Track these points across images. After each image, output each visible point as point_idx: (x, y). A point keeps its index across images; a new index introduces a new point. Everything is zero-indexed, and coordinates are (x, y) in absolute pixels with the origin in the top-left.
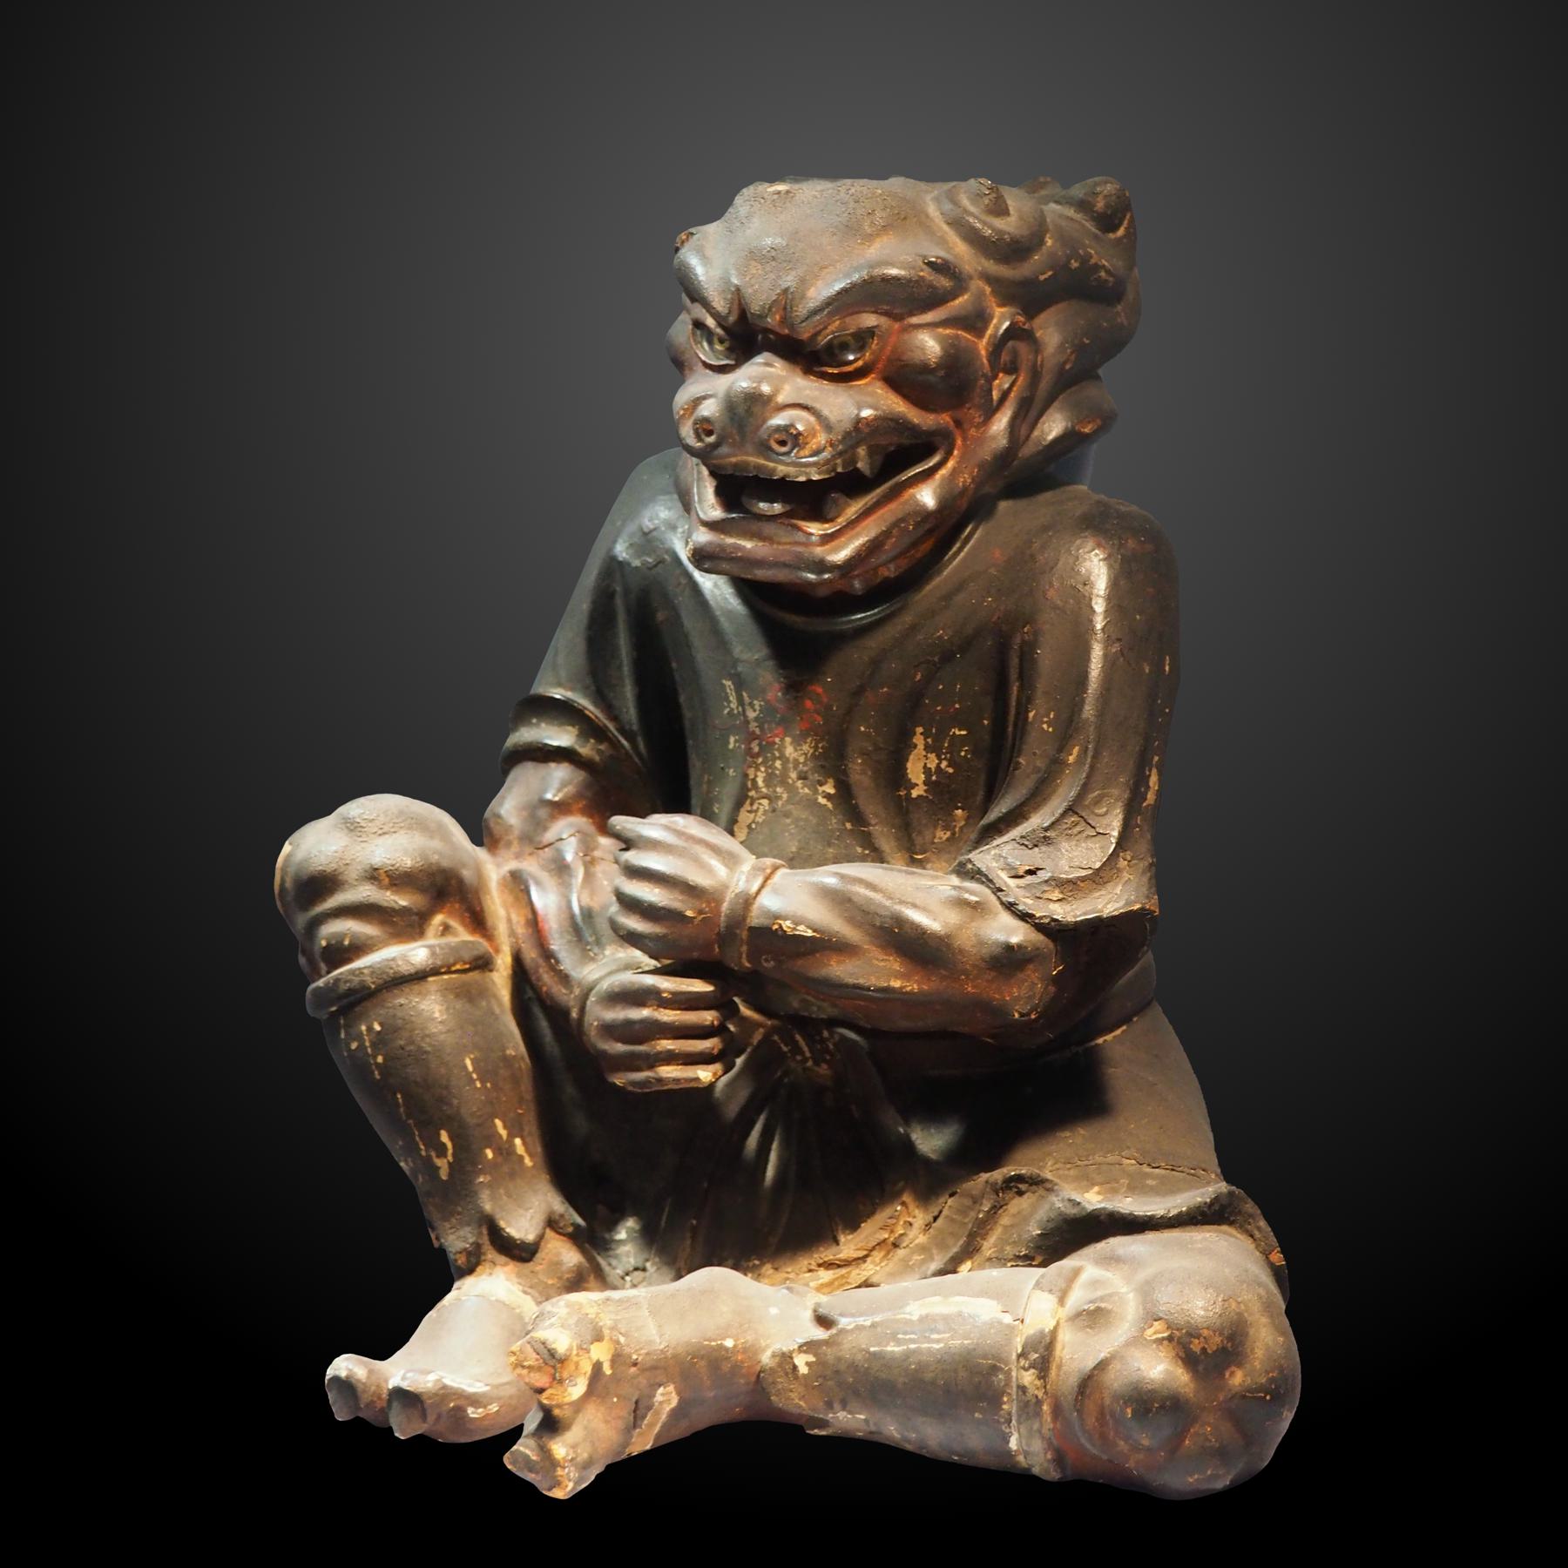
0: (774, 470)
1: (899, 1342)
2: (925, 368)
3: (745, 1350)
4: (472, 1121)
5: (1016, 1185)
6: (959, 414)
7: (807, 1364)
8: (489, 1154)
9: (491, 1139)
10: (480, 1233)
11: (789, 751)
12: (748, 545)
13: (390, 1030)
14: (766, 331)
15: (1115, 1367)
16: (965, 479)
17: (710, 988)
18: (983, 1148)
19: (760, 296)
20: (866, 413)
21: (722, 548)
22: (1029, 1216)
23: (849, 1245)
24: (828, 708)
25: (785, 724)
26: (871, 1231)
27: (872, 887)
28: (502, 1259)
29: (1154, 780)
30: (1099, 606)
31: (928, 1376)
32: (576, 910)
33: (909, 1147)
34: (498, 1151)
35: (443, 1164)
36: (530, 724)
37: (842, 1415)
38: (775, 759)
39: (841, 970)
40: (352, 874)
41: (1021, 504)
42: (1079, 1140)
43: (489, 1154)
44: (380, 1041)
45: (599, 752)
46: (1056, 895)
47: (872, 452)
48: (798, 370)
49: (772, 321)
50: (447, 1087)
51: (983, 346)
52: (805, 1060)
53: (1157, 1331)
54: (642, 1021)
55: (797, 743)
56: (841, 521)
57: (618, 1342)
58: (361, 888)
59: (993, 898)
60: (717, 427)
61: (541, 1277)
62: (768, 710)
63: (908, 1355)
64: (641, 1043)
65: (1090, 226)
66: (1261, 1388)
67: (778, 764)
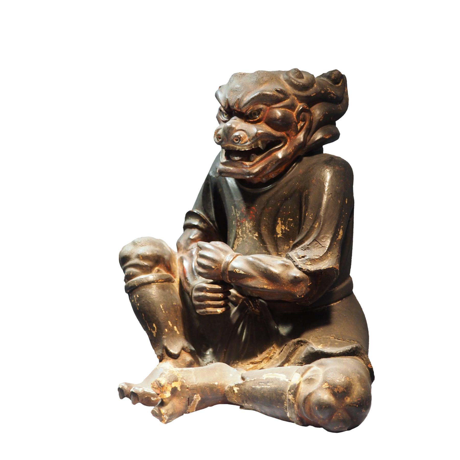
0: (236, 148)
1: (259, 385)
2: (276, 119)
3: (221, 386)
4: (161, 321)
5: (300, 343)
6: (288, 132)
7: (237, 390)
8: (166, 330)
9: (167, 326)
10: (163, 351)
11: (247, 225)
13: (141, 297)
14: (235, 110)
16: (290, 150)
17: (220, 287)
18: (294, 334)
19: (232, 102)
20: (260, 131)
21: (225, 170)
22: (303, 351)
23: (257, 359)
24: (256, 213)
26: (265, 354)
27: (260, 260)
28: (169, 358)
29: (341, 232)
30: (327, 185)
31: (266, 395)
32: (193, 267)
33: (278, 332)
34: (169, 330)
35: (154, 332)
37: (246, 404)
38: (243, 227)
39: (251, 283)
40: (133, 256)
41: (310, 158)
42: (320, 331)
43: (166, 330)
45: (204, 226)
46: (309, 263)
47: (262, 142)
48: (243, 121)
49: (236, 107)
50: (155, 313)
51: (294, 114)
52: (252, 308)
53: (326, 385)
54: (202, 296)
55: (249, 223)
56: (255, 161)
57: (183, 382)
59: (293, 264)
60: (221, 137)
61: (180, 363)
62: (242, 214)
63: (262, 389)
64: (202, 302)
65: (330, 83)
66: (355, 403)
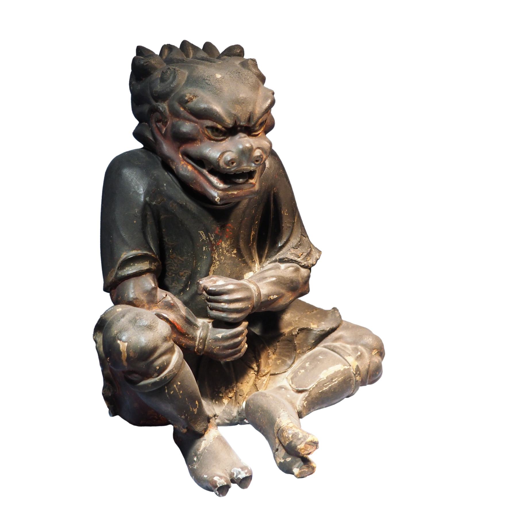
1: (326, 387)
11: (224, 245)
12: (235, 193)
15: (371, 364)
24: (234, 229)
25: (221, 238)
35: (195, 410)
36: (130, 266)
38: (220, 249)
40: (160, 342)
44: (181, 387)
45: (155, 266)
55: (225, 243)
58: (164, 345)
62: (216, 236)
63: (330, 388)
67: (221, 250)
